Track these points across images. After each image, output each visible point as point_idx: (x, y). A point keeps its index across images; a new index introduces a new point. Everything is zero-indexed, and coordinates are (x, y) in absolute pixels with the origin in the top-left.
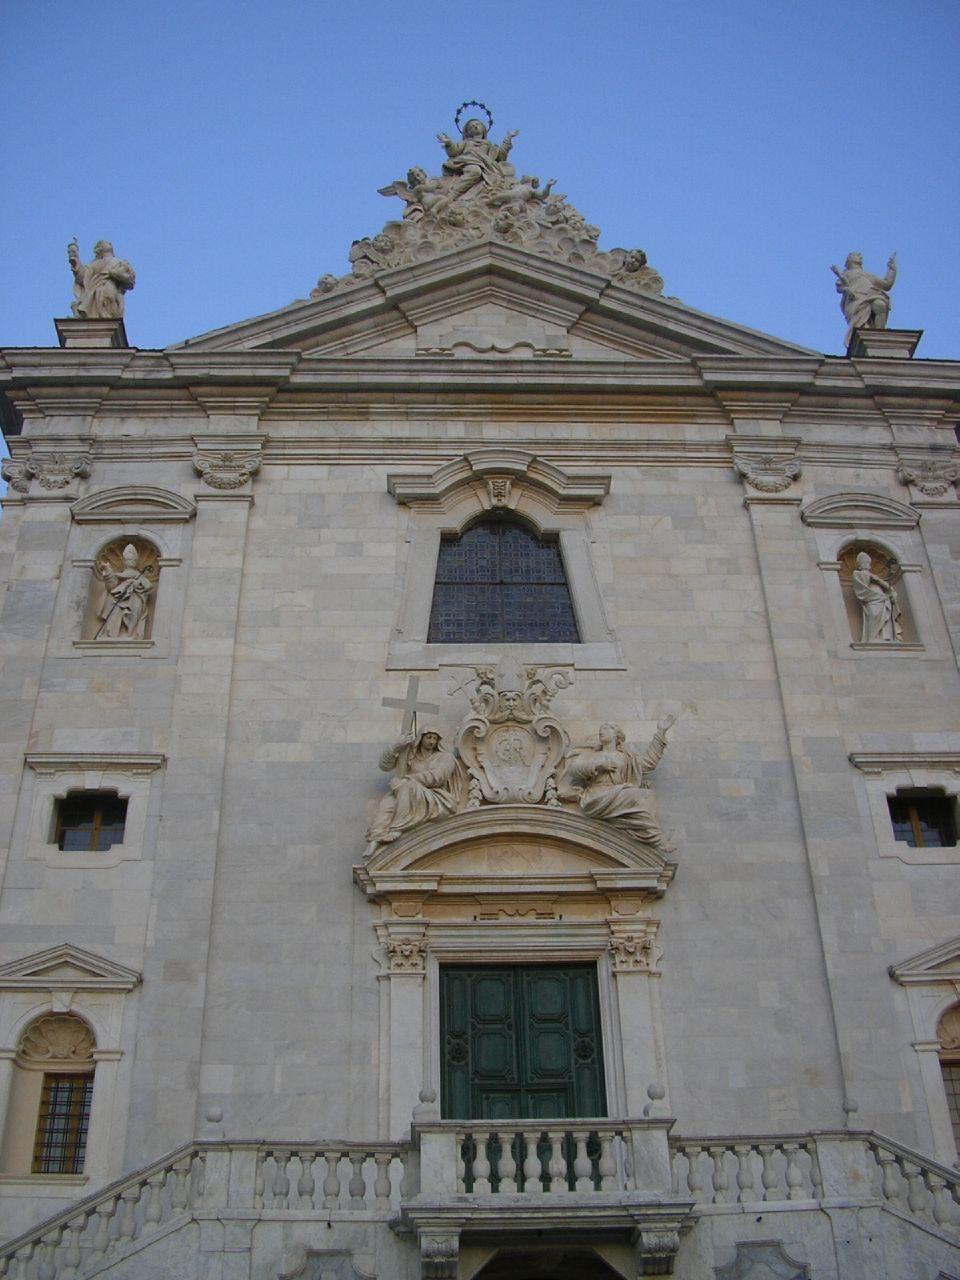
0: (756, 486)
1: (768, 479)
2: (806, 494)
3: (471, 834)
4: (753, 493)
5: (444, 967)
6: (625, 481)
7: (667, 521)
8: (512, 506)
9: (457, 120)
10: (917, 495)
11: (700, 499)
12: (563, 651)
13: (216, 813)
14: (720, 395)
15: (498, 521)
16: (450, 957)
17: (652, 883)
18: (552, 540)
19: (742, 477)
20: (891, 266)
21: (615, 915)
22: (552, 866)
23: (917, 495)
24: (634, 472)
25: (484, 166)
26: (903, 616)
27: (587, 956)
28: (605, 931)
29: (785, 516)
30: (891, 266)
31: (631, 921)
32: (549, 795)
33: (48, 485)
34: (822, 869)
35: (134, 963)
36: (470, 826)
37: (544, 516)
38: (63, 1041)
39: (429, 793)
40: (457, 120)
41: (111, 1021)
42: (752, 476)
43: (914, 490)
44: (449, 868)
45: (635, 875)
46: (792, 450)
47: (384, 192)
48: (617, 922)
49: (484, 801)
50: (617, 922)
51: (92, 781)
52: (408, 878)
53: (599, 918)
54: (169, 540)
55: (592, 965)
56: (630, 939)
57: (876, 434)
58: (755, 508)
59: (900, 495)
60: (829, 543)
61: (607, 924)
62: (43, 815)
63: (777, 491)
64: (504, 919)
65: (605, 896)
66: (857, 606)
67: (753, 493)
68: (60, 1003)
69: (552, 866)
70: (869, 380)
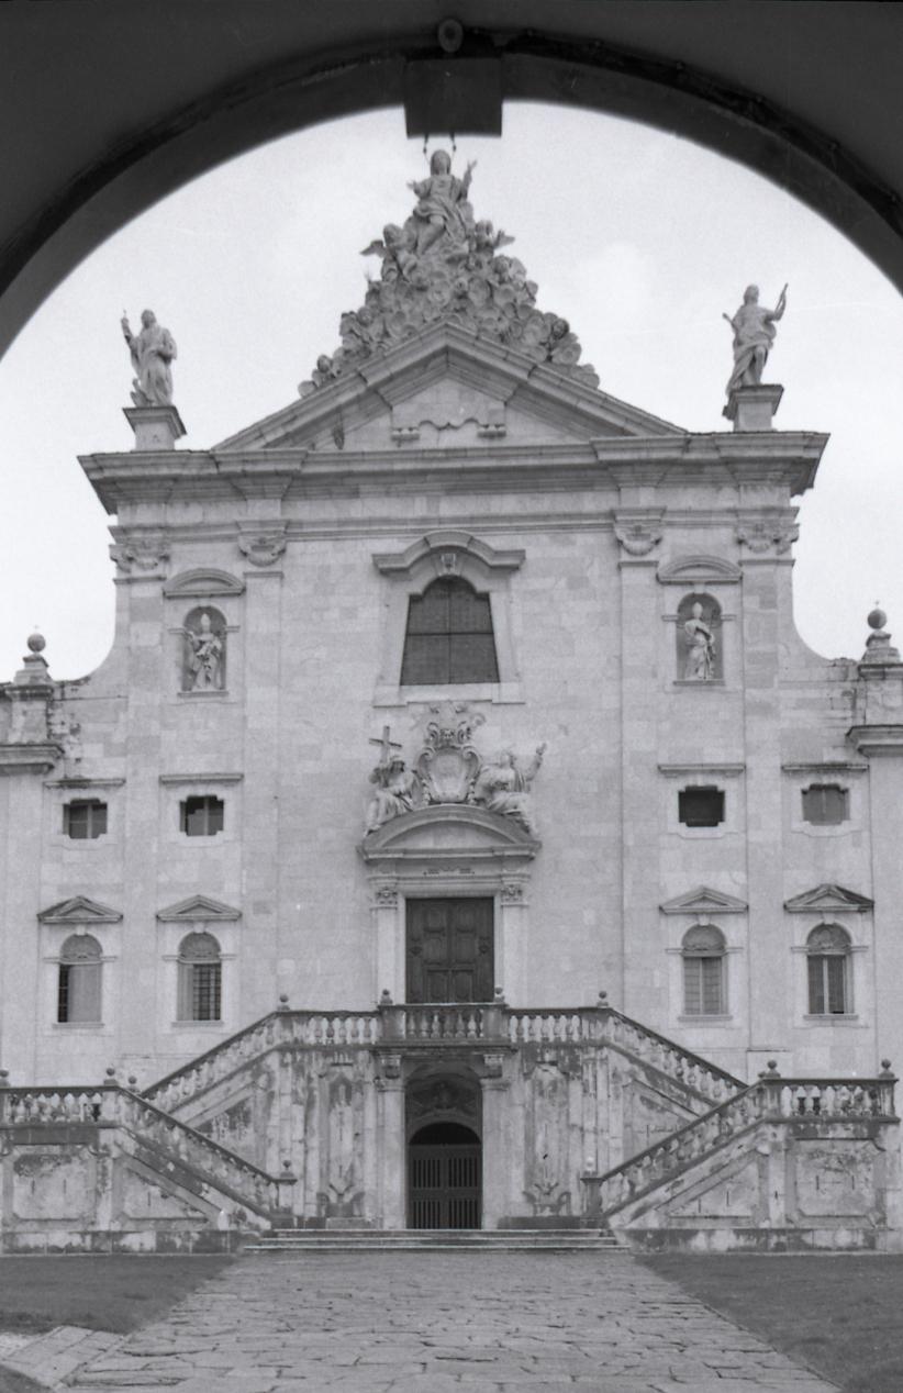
0: (629, 551)
1: (638, 545)
2: (664, 557)
4: (625, 557)
6: (538, 548)
7: (563, 583)
9: (425, 151)
10: (746, 554)
12: (486, 690)
14: (611, 469)
15: (449, 586)
16: (411, 895)
17: (526, 853)
18: (485, 598)
19: (620, 543)
21: (505, 871)
22: (469, 842)
23: (746, 554)
24: (544, 538)
26: (715, 657)
27: (489, 894)
28: (498, 880)
29: (643, 577)
31: (511, 876)
32: (470, 796)
33: (142, 566)
34: (630, 842)
35: (235, 904)
37: (480, 585)
38: (203, 945)
39: (397, 801)
40: (425, 151)
41: (227, 939)
42: (626, 542)
43: (745, 549)
44: (409, 844)
45: (517, 848)
46: (658, 517)
47: (367, 252)
49: (432, 802)
51: (201, 791)
53: (497, 872)
54: (230, 609)
55: (491, 899)
56: (512, 886)
57: (727, 498)
58: (626, 572)
59: (733, 555)
60: (674, 597)
61: (500, 876)
62: (174, 812)
63: (643, 553)
64: (442, 874)
65: (500, 860)
66: (684, 648)
67: (625, 557)
68: (199, 928)
69: (469, 842)
70: (724, 453)
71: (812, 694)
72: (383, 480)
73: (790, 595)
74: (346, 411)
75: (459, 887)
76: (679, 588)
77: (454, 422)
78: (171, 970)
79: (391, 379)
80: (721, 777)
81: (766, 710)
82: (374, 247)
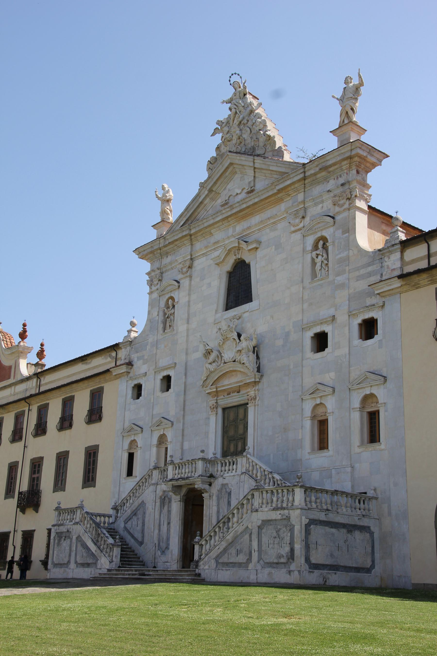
1: (297, 221)
3: (222, 373)
5: (224, 409)
8: (240, 257)
11: (282, 235)
13: (184, 377)
16: (224, 407)
20: (360, 77)
25: (235, 107)
30: (360, 77)
36: (221, 371)
47: (212, 135)
48: (248, 392)
50: (248, 392)
52: (211, 389)
60: (310, 241)
71: (363, 272)
72: (215, 226)
73: (355, 224)
74: (205, 202)
75: (237, 400)
76: (312, 236)
77: (239, 192)
78: (154, 450)
79: (215, 183)
80: (326, 325)
81: (342, 286)
82: (216, 131)
